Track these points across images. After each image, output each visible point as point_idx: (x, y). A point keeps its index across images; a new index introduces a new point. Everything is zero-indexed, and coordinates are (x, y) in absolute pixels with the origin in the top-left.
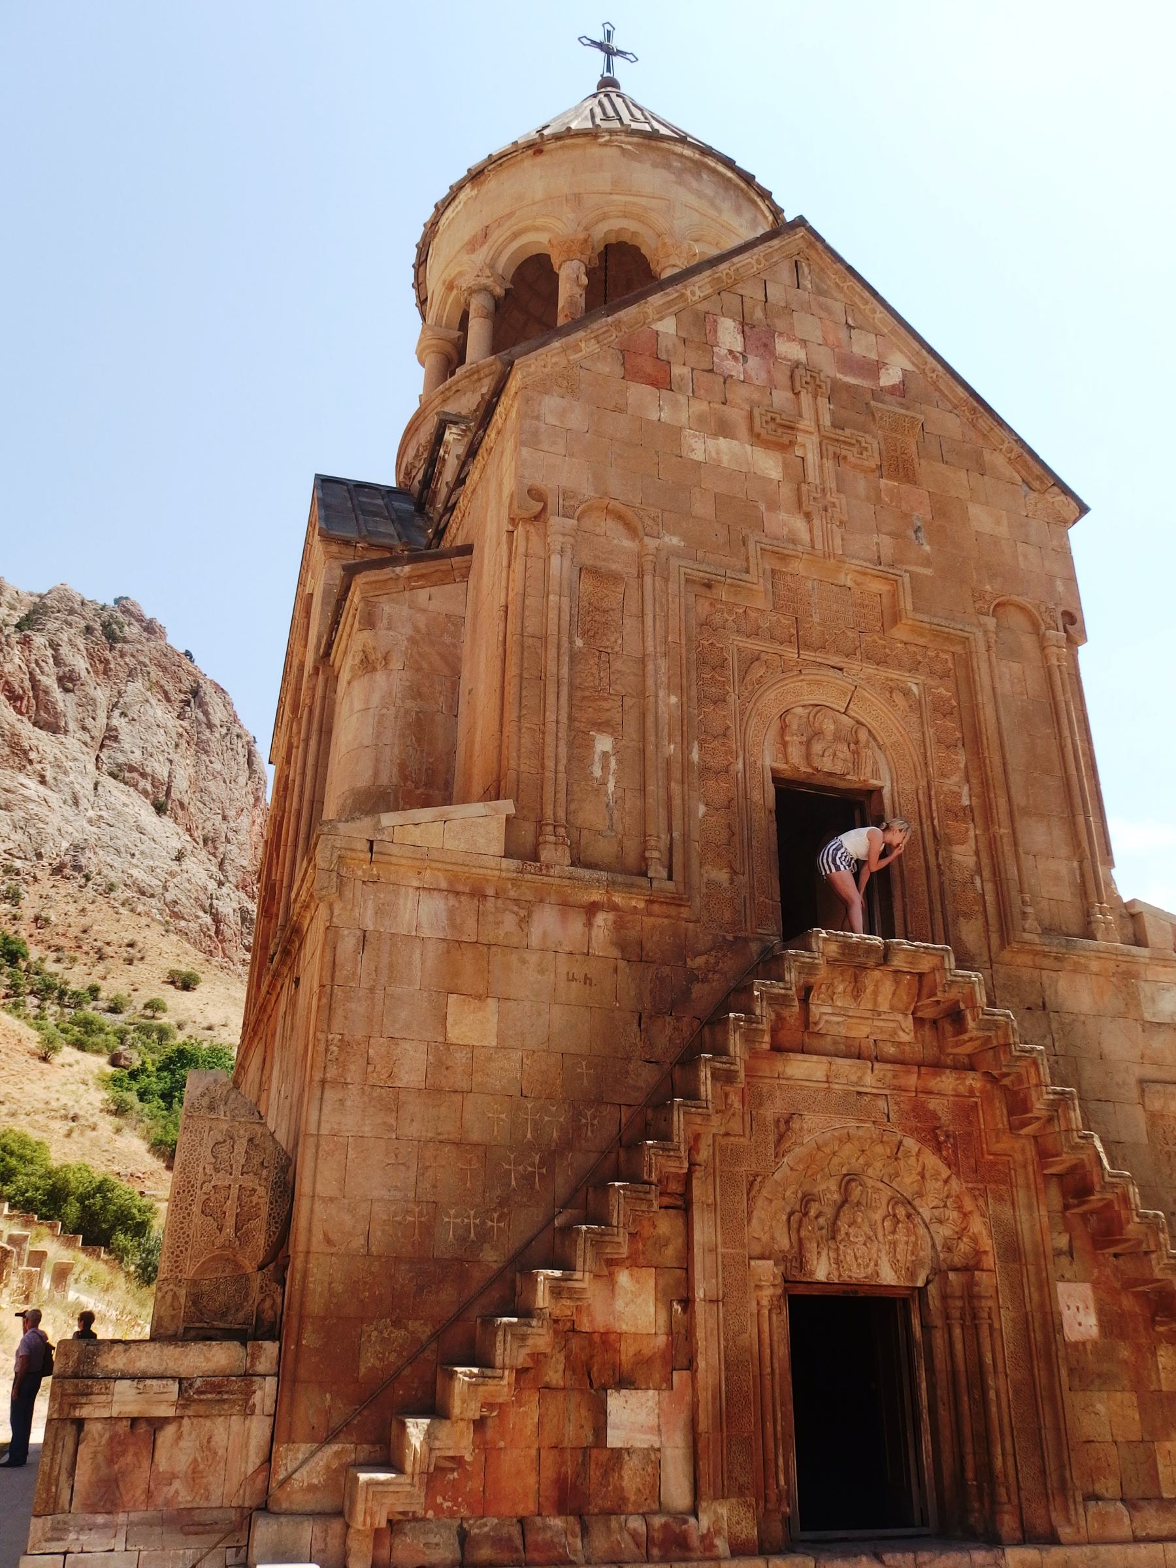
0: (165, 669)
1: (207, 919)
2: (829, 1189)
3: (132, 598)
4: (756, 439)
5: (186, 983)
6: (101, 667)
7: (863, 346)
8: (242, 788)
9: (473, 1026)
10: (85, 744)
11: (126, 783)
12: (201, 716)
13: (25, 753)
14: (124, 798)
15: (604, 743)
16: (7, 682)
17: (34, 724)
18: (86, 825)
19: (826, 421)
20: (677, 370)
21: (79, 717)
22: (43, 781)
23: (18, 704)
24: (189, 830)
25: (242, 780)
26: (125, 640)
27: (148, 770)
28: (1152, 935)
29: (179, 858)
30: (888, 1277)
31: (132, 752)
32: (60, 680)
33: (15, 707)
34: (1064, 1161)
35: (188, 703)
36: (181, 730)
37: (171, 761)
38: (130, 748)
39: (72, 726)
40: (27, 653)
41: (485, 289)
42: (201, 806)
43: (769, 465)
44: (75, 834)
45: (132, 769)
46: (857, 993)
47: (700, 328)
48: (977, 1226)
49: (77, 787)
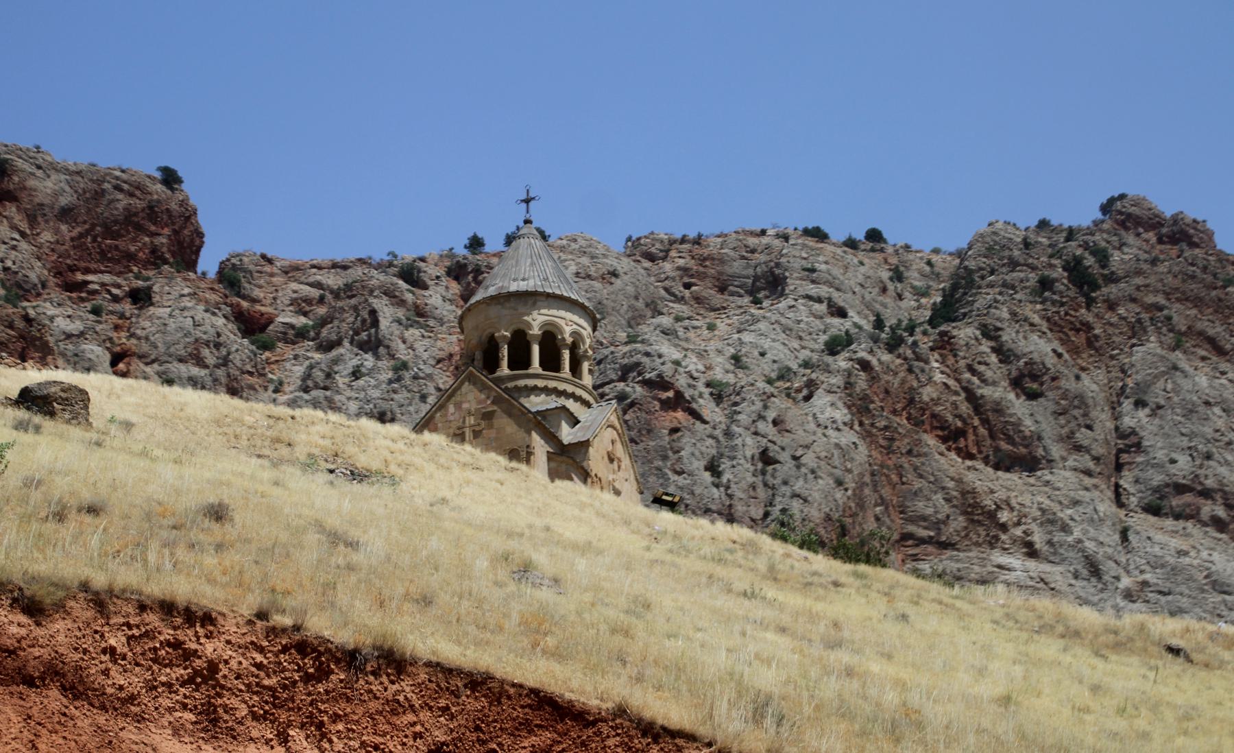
0: (1198, 302)
3: (1131, 192)
6: (1079, 339)
10: (1088, 473)
11: (1177, 517)
13: (992, 515)
14: (1176, 543)
16: (934, 416)
17: (997, 467)
21: (1064, 431)
23: (962, 443)
27: (1210, 483)
31: (1173, 461)
32: (1016, 383)
33: (959, 451)
38: (1167, 454)
39: (1056, 451)
45: (1180, 489)
49: (1090, 546)
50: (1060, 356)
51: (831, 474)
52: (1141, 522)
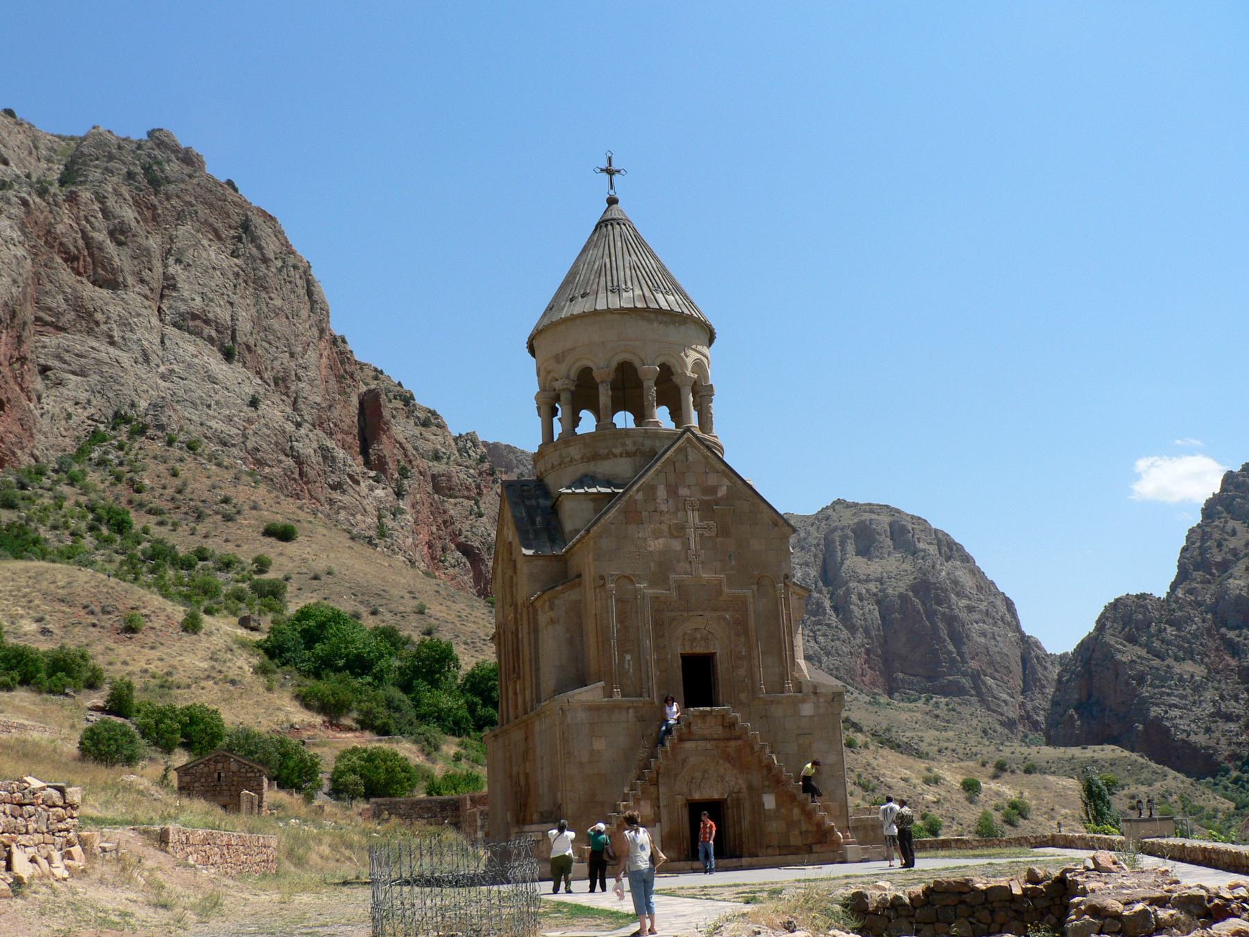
0: (211, 206)
1: (289, 462)
2: (698, 775)
3: (166, 128)
4: (672, 536)
5: (284, 534)
6: (148, 214)
7: (712, 480)
8: (305, 321)
9: (599, 745)
10: (146, 297)
11: (190, 333)
12: (255, 251)
13: (91, 315)
15: (628, 657)
16: (61, 244)
17: (94, 283)
18: (160, 381)
19: (697, 520)
20: (644, 514)
21: (136, 269)
22: (112, 343)
23: (75, 264)
24: (258, 373)
25: (304, 313)
26: (168, 181)
27: (210, 316)
28: (804, 688)
29: (254, 403)
30: (716, 796)
31: (193, 300)
32: (111, 234)
33: (72, 268)
34: (765, 762)
35: (240, 239)
36: (236, 269)
37: (231, 304)
38: (190, 295)
39: (130, 280)
40: (75, 211)
41: (567, 389)
42: (267, 346)
43: (677, 545)
44: (151, 392)
45: (194, 317)
46: (704, 722)
47: (651, 490)
48: (740, 781)
50: (138, 222)
51: (10, 275)
52: (171, 331)
